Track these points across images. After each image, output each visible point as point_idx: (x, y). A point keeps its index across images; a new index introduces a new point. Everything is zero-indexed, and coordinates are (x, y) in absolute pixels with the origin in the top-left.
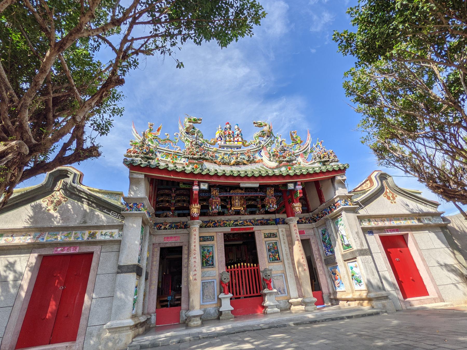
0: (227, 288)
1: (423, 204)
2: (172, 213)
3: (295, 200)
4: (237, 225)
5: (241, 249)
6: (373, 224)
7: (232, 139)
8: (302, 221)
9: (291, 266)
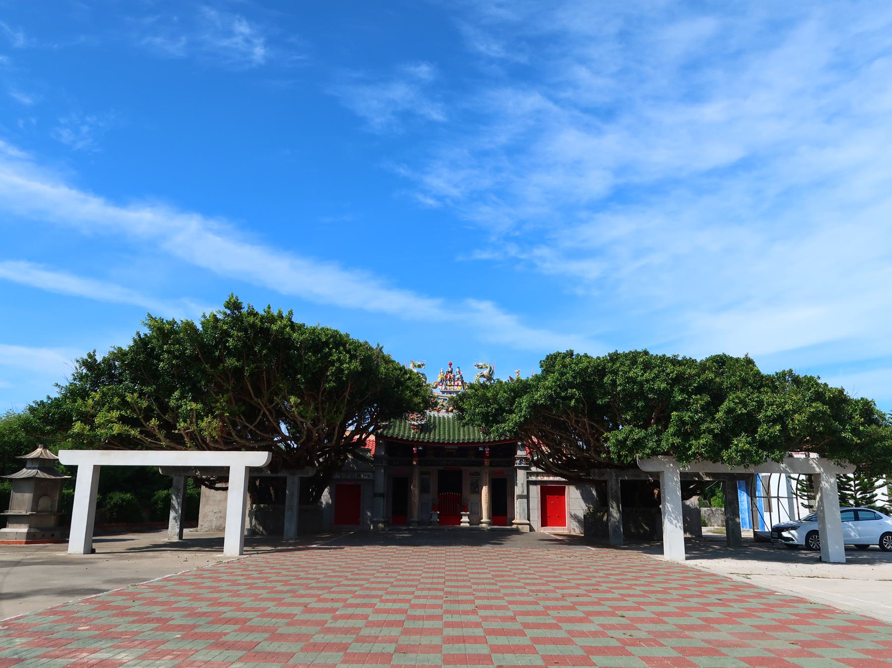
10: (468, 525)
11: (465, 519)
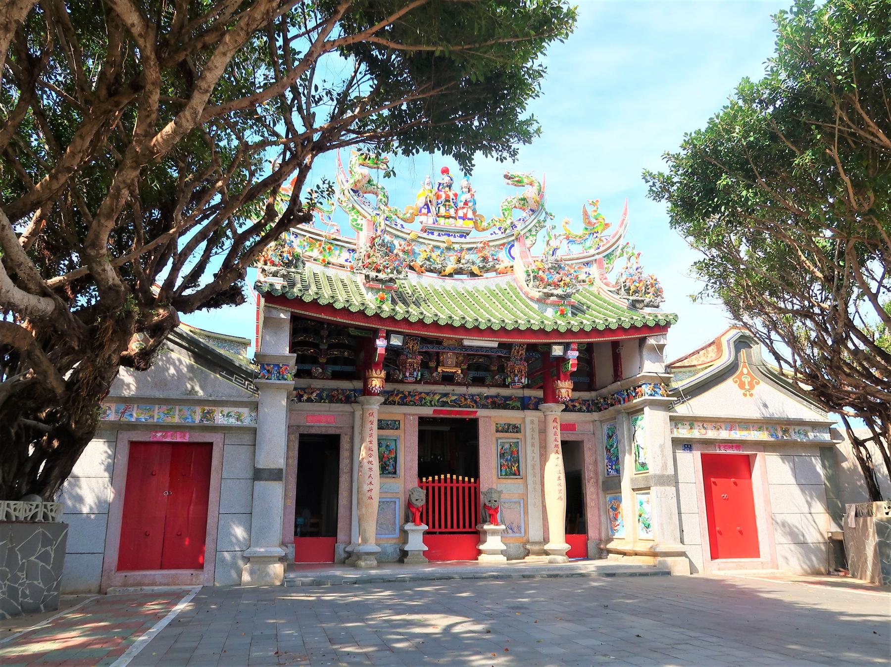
0: (418, 515)
1: (805, 403)
2: (320, 370)
3: (562, 376)
4: (444, 404)
5: (449, 449)
6: (696, 433)
7: (452, 212)
8: (574, 406)
9: (539, 487)
10: (502, 559)
11: (493, 543)
